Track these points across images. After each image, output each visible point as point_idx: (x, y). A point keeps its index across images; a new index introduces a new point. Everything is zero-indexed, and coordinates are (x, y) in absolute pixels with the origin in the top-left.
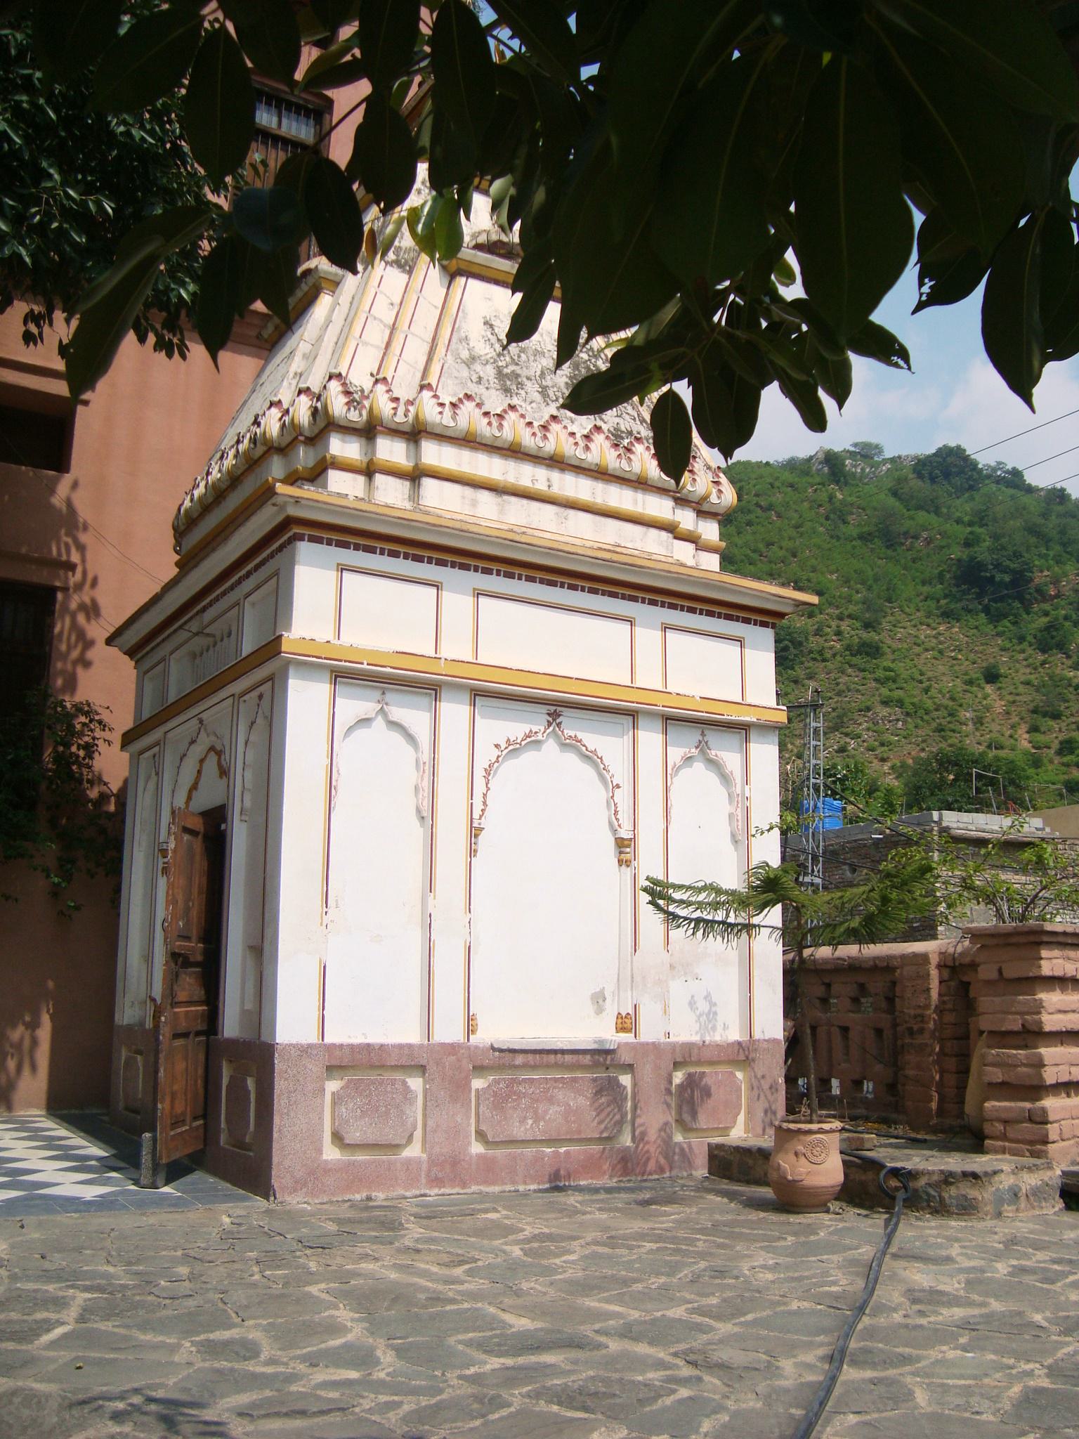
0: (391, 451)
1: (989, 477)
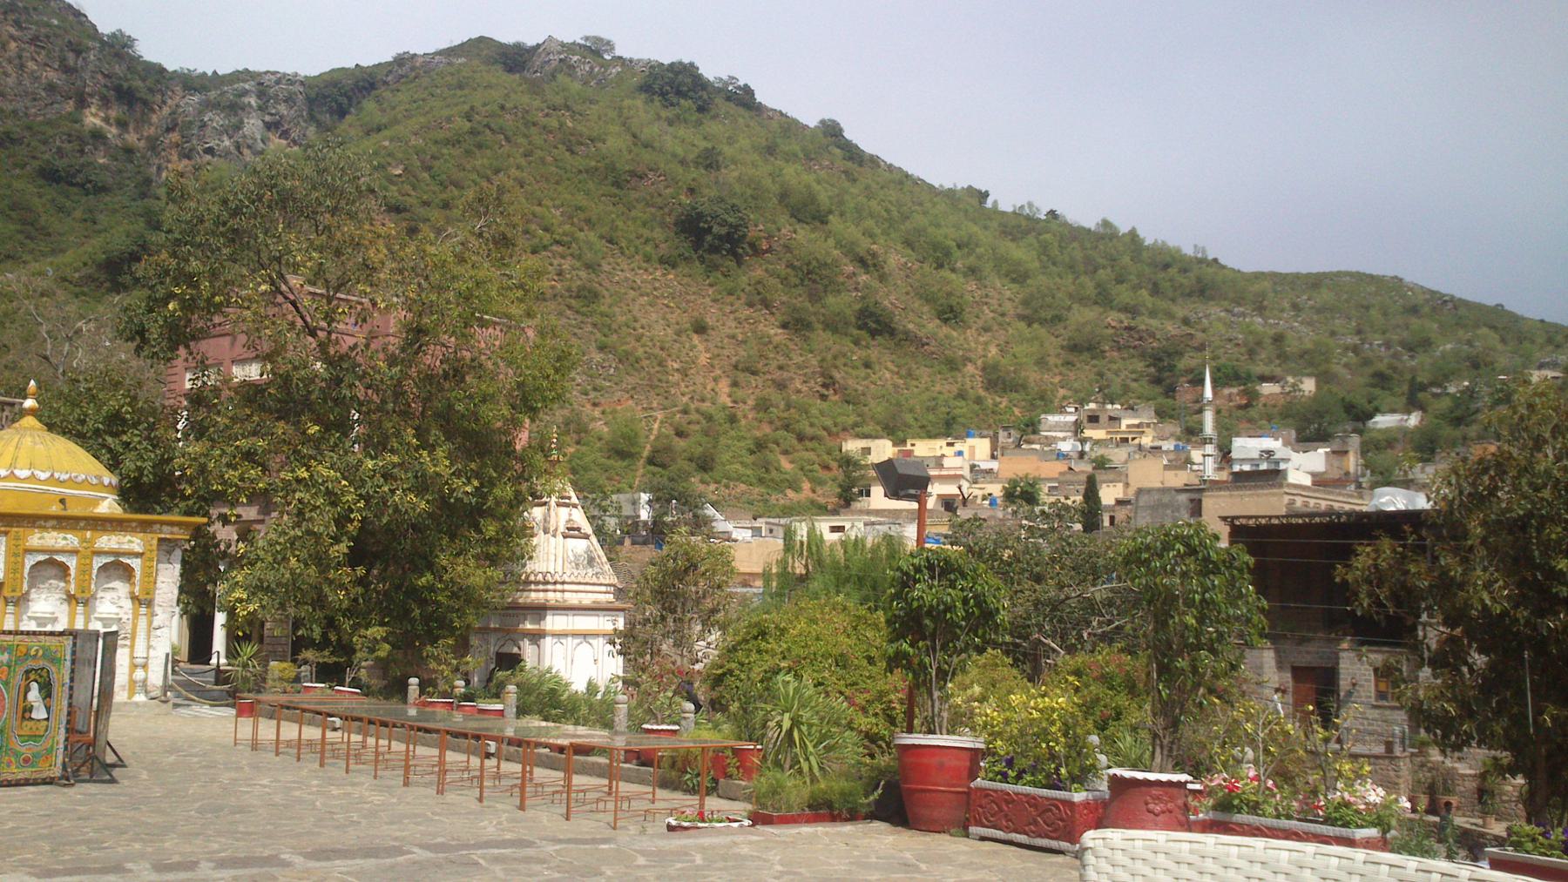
0: (559, 587)
1: (719, 90)
